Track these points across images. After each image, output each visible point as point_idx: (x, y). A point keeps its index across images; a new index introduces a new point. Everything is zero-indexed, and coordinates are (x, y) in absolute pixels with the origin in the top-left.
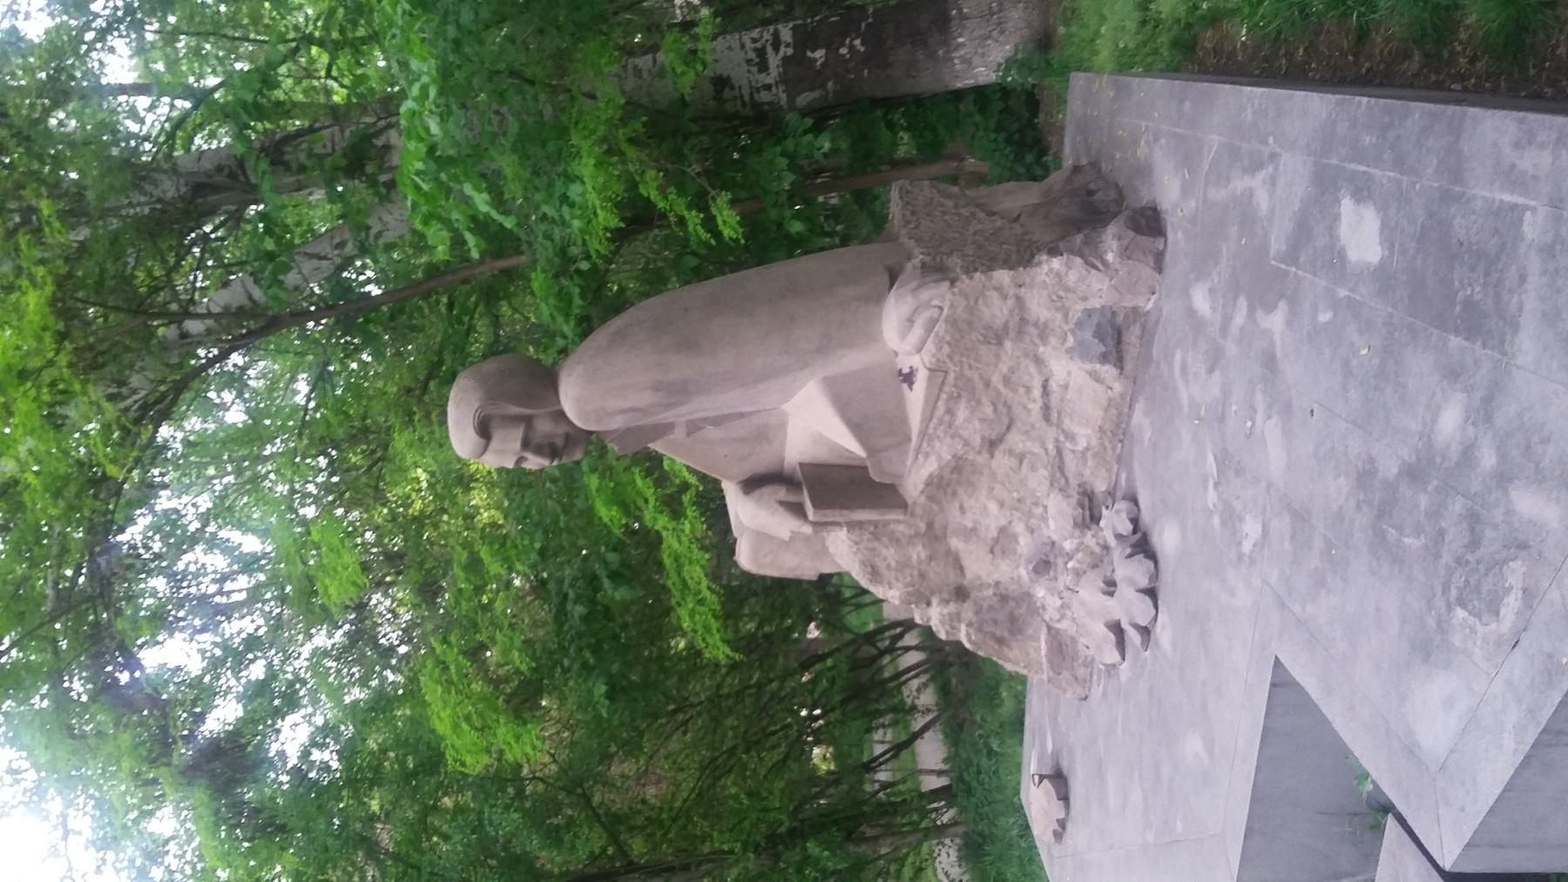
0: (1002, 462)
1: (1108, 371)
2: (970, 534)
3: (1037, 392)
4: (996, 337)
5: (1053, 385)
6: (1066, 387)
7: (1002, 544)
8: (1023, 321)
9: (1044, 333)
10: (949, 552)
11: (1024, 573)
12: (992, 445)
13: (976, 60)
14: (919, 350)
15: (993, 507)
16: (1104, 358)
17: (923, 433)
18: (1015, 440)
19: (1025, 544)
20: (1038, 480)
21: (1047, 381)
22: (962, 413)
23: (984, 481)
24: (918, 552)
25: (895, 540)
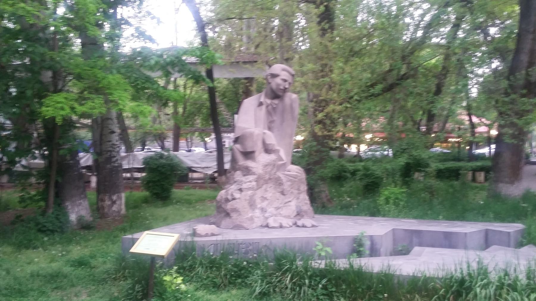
0: (278, 195)
1: (295, 213)
2: (266, 191)
3: (290, 200)
4: (299, 189)
5: (290, 203)
6: (289, 206)
7: (264, 199)
8: (299, 193)
9: (298, 198)
10: (263, 185)
11: (259, 206)
12: (283, 193)
13: (80, 207)
14: (297, 172)
15: (270, 195)
16: (297, 212)
17: (287, 175)
18: (282, 196)
19: (264, 204)
20: (276, 204)
21: (290, 201)
22: (289, 183)
23: (274, 192)
24: (267, 177)
25: (272, 169)
